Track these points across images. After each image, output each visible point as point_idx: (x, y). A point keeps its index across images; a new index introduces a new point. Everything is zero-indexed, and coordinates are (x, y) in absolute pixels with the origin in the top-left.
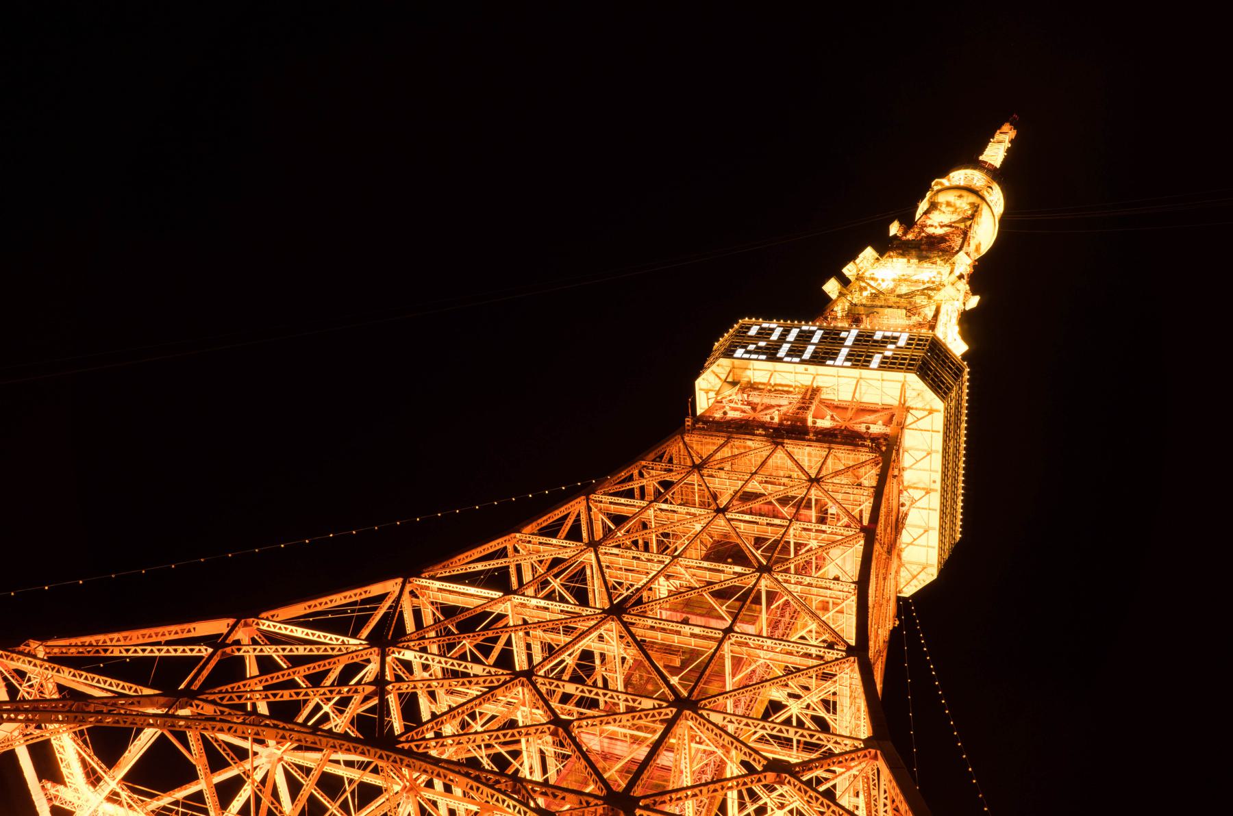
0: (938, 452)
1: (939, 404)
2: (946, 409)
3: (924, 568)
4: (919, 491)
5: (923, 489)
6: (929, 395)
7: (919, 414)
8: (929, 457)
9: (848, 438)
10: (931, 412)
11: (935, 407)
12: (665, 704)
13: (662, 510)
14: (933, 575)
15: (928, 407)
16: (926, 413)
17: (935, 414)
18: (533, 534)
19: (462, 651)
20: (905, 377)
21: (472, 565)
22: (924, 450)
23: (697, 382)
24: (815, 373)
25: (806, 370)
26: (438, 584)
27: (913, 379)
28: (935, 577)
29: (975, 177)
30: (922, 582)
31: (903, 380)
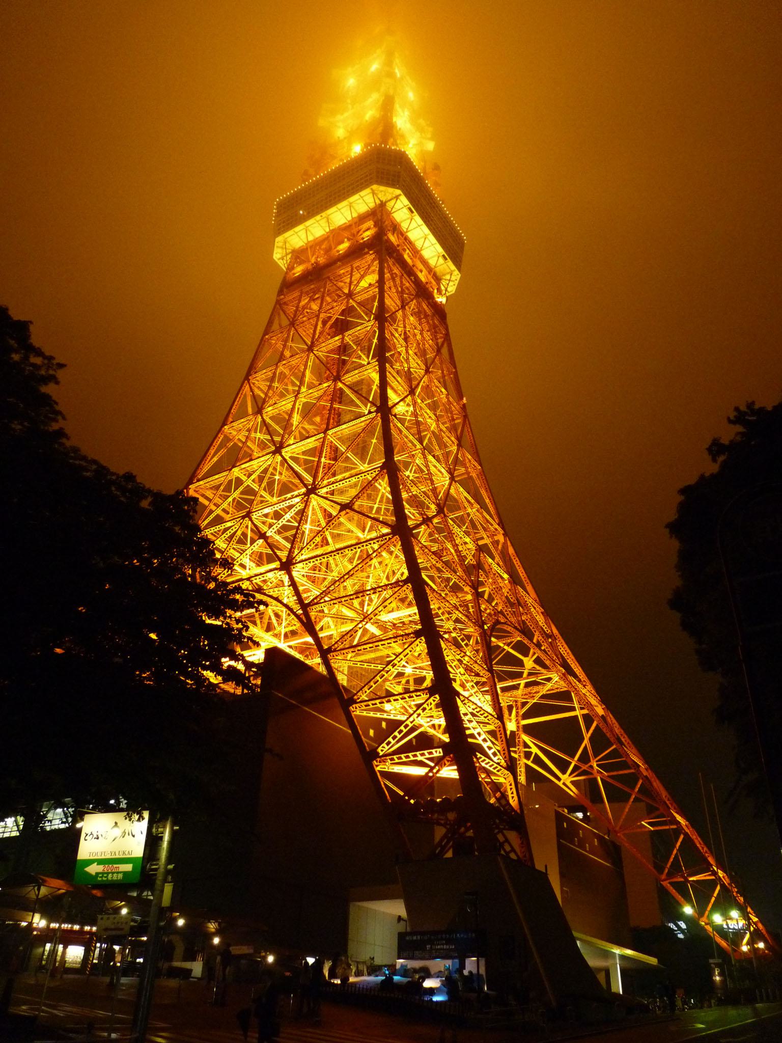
1: (398, 192)
3: (451, 275)
4: (421, 240)
5: (421, 238)
6: (391, 190)
7: (393, 202)
8: (413, 220)
9: (357, 251)
10: (397, 197)
12: (303, 496)
13: (284, 364)
15: (394, 196)
16: (395, 200)
18: (232, 422)
19: (236, 501)
20: (372, 189)
21: (212, 461)
22: (408, 219)
23: (274, 257)
25: (321, 216)
26: (201, 483)
27: (375, 187)
31: (371, 191)
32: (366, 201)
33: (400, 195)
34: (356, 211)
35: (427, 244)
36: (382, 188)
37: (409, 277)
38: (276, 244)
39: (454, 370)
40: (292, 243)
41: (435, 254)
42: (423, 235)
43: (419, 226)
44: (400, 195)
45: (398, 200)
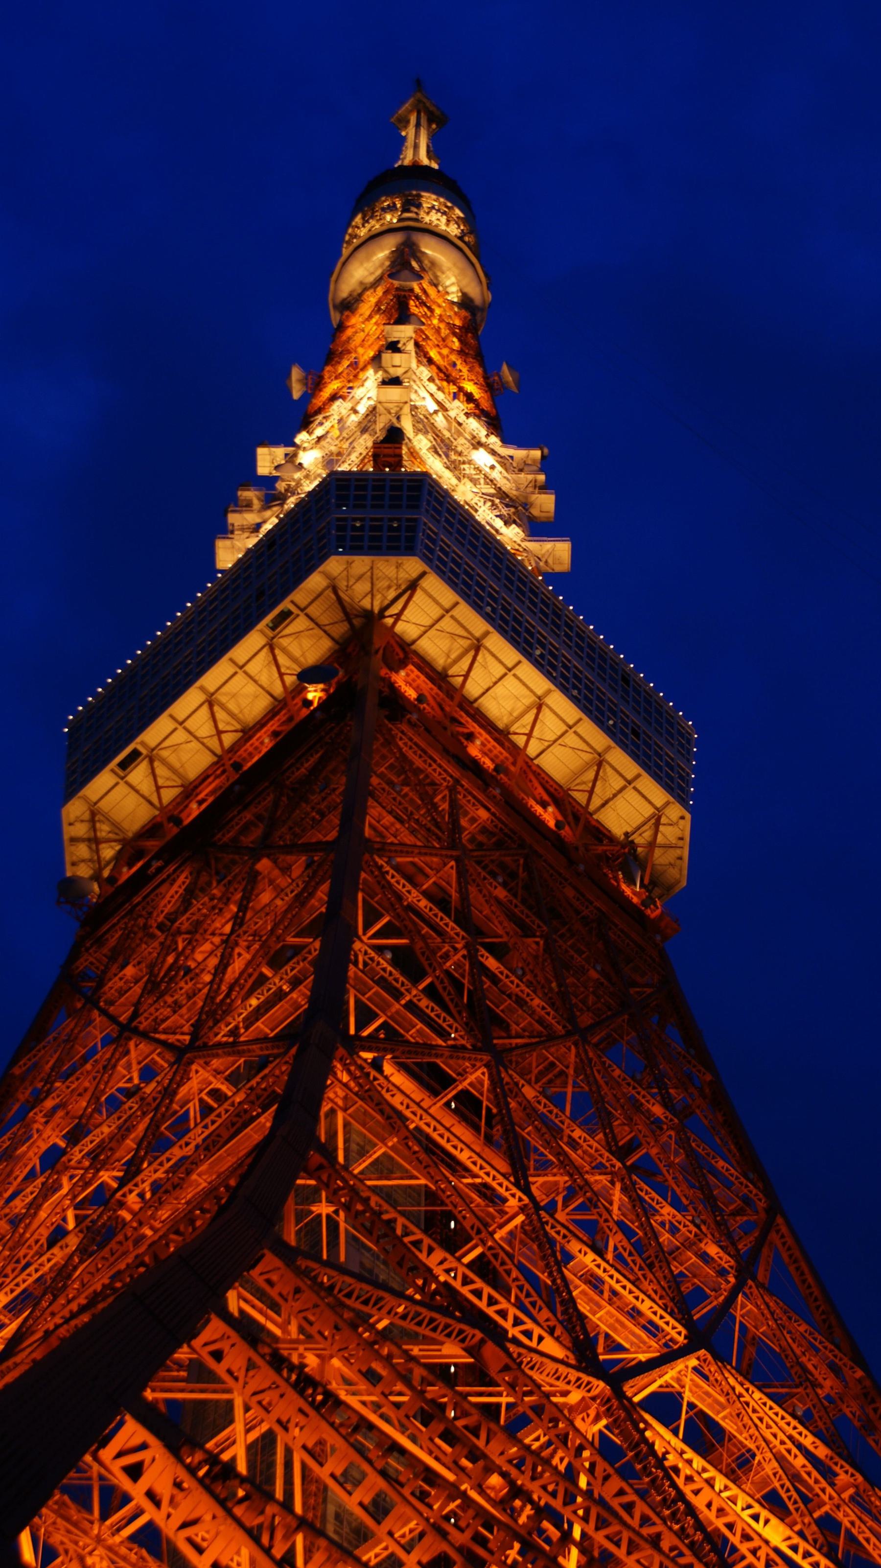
0: (487, 634)
1: (413, 566)
2: (428, 561)
3: (659, 819)
10: (413, 586)
11: (414, 575)
14: (682, 818)
17: (426, 583)
24: (201, 698)
28: (688, 816)
29: (422, 214)
30: (680, 843)
32: (321, 623)
33: (423, 575)
34: (294, 660)
35: (550, 726)
36: (361, 563)
37: (484, 791)
38: (69, 832)
39: (708, 1077)
40: (118, 816)
41: (587, 757)
42: (529, 699)
43: (510, 670)
44: (423, 575)
45: (419, 595)
